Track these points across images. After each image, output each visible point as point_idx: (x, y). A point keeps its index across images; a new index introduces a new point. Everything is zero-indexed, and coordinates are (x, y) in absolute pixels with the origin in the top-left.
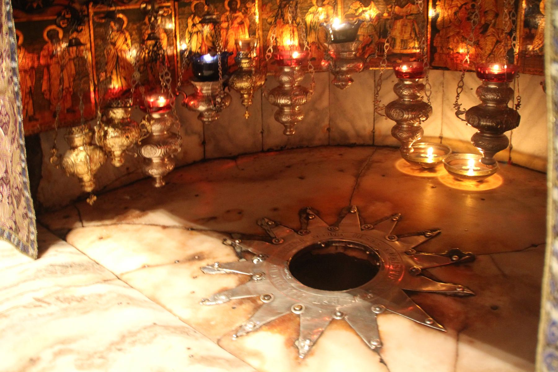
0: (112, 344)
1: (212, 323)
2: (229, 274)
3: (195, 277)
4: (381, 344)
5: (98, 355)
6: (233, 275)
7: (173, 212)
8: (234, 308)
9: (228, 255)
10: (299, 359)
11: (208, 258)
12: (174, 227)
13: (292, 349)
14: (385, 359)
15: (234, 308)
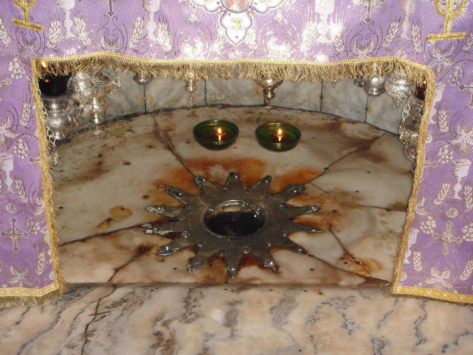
0: (186, 307)
1: (211, 277)
3: (163, 261)
5: (188, 314)
8: (211, 265)
9: (162, 239)
10: (276, 270)
14: (311, 254)
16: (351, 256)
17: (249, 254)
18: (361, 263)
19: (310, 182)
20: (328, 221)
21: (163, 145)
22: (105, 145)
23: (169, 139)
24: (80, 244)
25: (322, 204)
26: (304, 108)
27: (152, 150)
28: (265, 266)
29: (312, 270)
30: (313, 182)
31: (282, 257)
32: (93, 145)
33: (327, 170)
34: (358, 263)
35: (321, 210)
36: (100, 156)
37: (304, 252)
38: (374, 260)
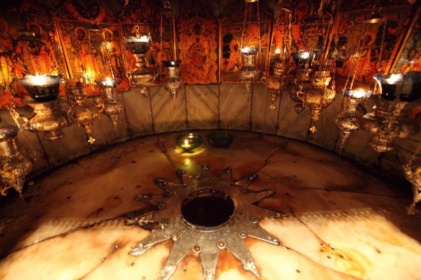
2: (154, 245)
3: (133, 264)
4: (278, 239)
6: (159, 246)
7: (58, 218)
8: (185, 270)
9: (139, 232)
11: (128, 242)
12: (72, 231)
13: (247, 273)
15: (185, 270)
16: (329, 245)
17: (226, 249)
18: (345, 256)
19: (259, 171)
20: (286, 204)
21: (159, 150)
22: (125, 151)
23: (164, 147)
24: (58, 239)
25: (275, 188)
26: (240, 129)
27: (152, 153)
28: (246, 268)
29: (298, 271)
30: (261, 170)
31: (261, 251)
32: (117, 152)
33: (267, 162)
34: (342, 257)
35: (276, 193)
36: (119, 157)
37: (280, 243)
38: (354, 251)
